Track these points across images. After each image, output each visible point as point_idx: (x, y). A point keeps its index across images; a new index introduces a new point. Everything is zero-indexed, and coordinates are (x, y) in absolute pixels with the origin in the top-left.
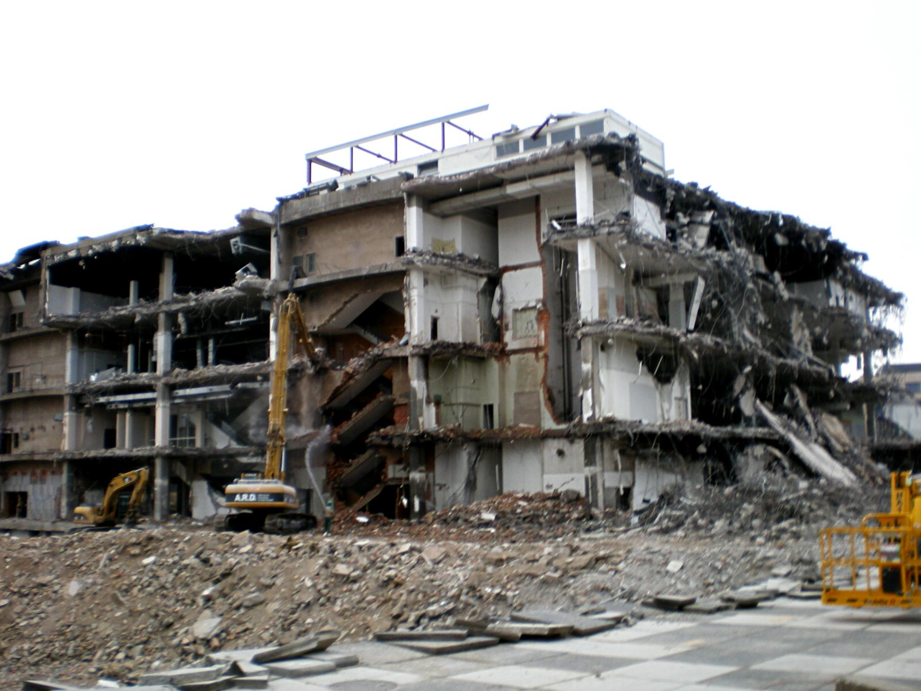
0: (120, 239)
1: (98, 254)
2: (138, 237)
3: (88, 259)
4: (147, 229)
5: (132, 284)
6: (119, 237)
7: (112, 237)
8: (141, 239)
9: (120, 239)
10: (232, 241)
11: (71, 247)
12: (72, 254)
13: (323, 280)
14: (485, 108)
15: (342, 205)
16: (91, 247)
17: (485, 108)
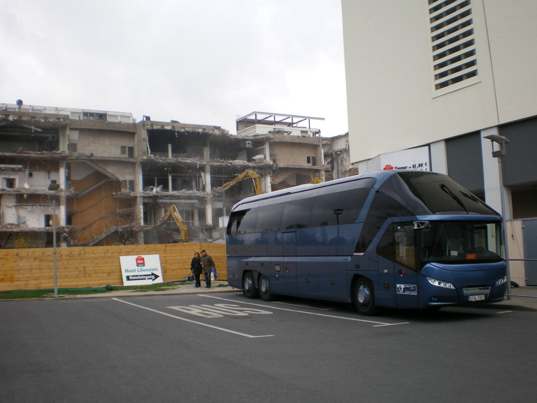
0: (204, 129)
1: (188, 132)
2: (216, 131)
3: (178, 132)
4: (218, 128)
5: (170, 146)
6: (204, 128)
7: (199, 127)
8: (217, 132)
9: (204, 129)
10: (247, 142)
11: (168, 124)
12: (169, 128)
13: (290, 167)
14: (323, 119)
15: (296, 141)
16: (184, 128)
17: (323, 119)
